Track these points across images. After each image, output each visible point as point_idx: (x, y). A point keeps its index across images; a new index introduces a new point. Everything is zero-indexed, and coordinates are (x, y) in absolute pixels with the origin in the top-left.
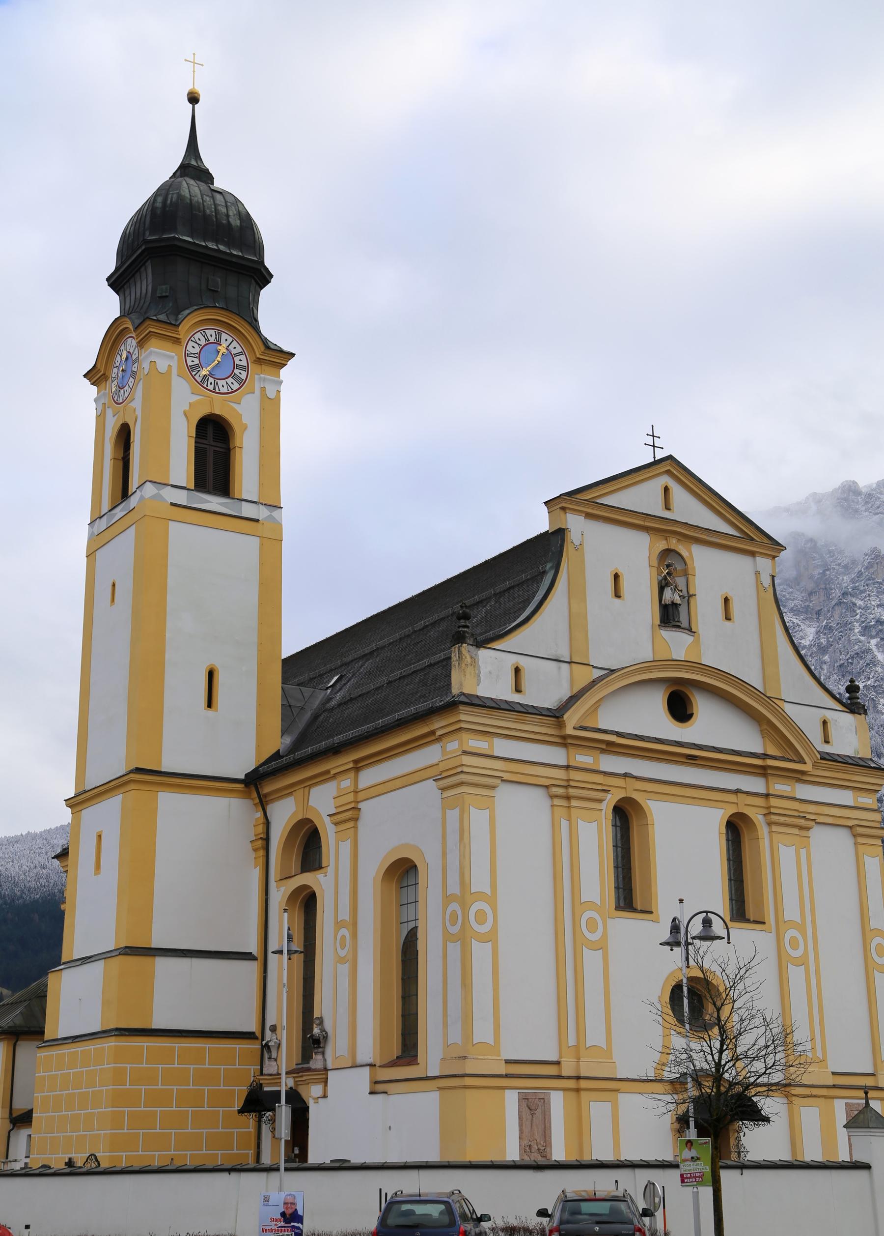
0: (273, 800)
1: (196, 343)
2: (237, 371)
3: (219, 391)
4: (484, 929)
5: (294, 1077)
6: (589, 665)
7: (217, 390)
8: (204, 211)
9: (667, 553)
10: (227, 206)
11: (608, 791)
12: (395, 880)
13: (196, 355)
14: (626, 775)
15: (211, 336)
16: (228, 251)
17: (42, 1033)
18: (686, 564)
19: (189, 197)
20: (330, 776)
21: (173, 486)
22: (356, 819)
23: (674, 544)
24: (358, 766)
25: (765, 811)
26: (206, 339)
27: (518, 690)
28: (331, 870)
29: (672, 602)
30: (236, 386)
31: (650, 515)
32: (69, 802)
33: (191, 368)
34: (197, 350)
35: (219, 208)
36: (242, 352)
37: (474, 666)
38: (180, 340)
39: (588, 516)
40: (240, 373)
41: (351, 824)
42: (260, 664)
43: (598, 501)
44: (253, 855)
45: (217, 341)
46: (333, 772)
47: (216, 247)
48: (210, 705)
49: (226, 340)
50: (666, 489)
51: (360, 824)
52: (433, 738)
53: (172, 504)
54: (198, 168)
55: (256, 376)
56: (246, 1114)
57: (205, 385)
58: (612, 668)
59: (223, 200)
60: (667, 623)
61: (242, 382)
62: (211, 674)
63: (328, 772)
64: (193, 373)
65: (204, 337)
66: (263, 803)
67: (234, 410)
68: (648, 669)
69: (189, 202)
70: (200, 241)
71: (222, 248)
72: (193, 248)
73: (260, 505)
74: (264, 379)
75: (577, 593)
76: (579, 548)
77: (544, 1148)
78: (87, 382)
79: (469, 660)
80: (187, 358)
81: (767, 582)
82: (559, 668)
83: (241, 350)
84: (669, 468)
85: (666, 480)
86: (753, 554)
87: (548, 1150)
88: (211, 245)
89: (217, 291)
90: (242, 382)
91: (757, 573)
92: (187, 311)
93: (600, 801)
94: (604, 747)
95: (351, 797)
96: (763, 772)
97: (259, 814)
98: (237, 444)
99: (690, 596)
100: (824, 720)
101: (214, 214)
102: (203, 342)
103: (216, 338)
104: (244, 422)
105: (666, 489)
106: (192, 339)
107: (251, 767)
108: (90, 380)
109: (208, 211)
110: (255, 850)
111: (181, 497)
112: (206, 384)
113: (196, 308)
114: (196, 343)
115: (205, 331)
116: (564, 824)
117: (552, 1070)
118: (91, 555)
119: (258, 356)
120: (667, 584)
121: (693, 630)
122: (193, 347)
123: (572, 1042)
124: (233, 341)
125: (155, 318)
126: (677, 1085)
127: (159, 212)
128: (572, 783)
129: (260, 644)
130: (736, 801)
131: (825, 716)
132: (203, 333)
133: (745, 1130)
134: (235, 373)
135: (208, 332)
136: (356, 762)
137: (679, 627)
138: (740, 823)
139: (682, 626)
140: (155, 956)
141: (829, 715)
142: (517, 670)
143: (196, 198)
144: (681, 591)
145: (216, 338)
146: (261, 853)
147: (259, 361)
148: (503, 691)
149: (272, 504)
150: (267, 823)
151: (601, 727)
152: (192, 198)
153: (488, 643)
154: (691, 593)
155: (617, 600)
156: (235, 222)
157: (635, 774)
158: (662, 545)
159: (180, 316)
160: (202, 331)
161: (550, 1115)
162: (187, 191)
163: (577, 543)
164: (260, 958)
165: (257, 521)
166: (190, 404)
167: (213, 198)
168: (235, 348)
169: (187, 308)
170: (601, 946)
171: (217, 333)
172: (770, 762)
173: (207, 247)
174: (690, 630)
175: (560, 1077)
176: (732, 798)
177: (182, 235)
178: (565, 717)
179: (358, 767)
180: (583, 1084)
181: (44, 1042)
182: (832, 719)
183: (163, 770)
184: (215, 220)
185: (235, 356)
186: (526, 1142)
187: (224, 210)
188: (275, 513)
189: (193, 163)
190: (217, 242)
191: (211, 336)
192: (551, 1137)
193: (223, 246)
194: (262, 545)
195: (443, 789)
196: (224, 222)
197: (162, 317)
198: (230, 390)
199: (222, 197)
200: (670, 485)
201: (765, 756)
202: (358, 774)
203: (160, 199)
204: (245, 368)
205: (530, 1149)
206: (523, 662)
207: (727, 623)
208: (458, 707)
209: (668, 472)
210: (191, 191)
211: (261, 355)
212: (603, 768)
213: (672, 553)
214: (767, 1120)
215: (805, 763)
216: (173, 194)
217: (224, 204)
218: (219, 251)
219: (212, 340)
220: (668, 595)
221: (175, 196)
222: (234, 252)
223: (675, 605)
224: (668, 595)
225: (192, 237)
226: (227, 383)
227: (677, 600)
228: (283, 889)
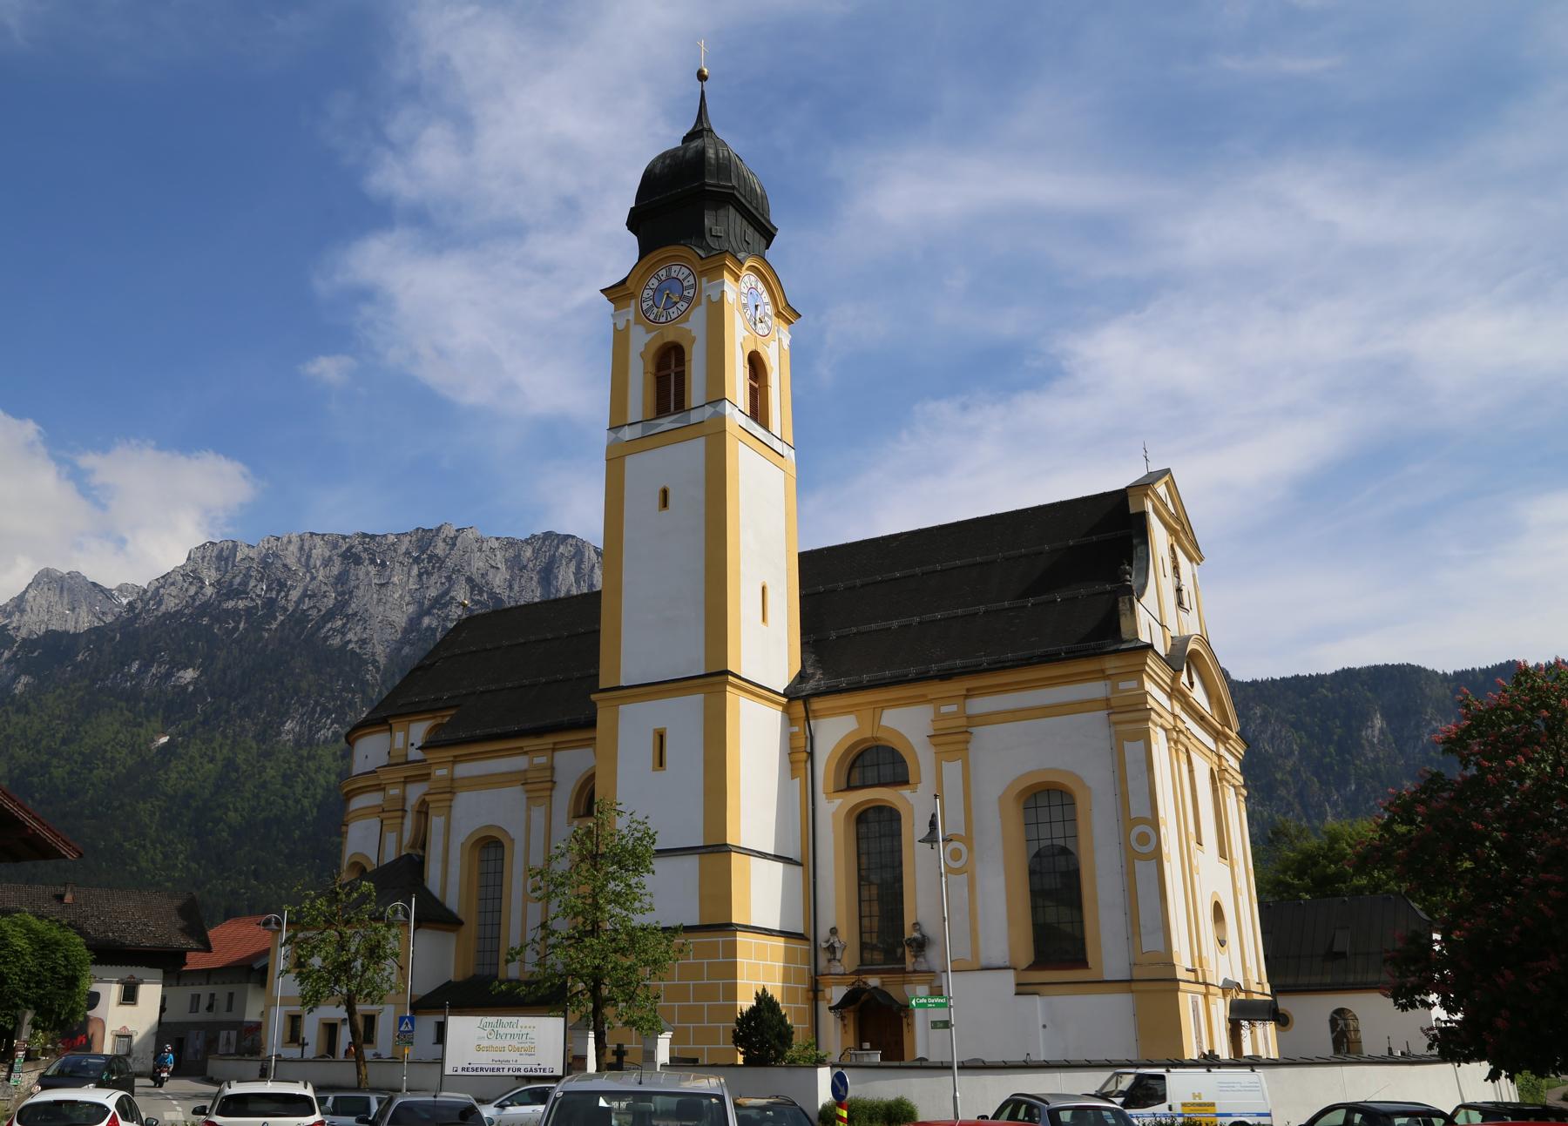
5: (882, 978)
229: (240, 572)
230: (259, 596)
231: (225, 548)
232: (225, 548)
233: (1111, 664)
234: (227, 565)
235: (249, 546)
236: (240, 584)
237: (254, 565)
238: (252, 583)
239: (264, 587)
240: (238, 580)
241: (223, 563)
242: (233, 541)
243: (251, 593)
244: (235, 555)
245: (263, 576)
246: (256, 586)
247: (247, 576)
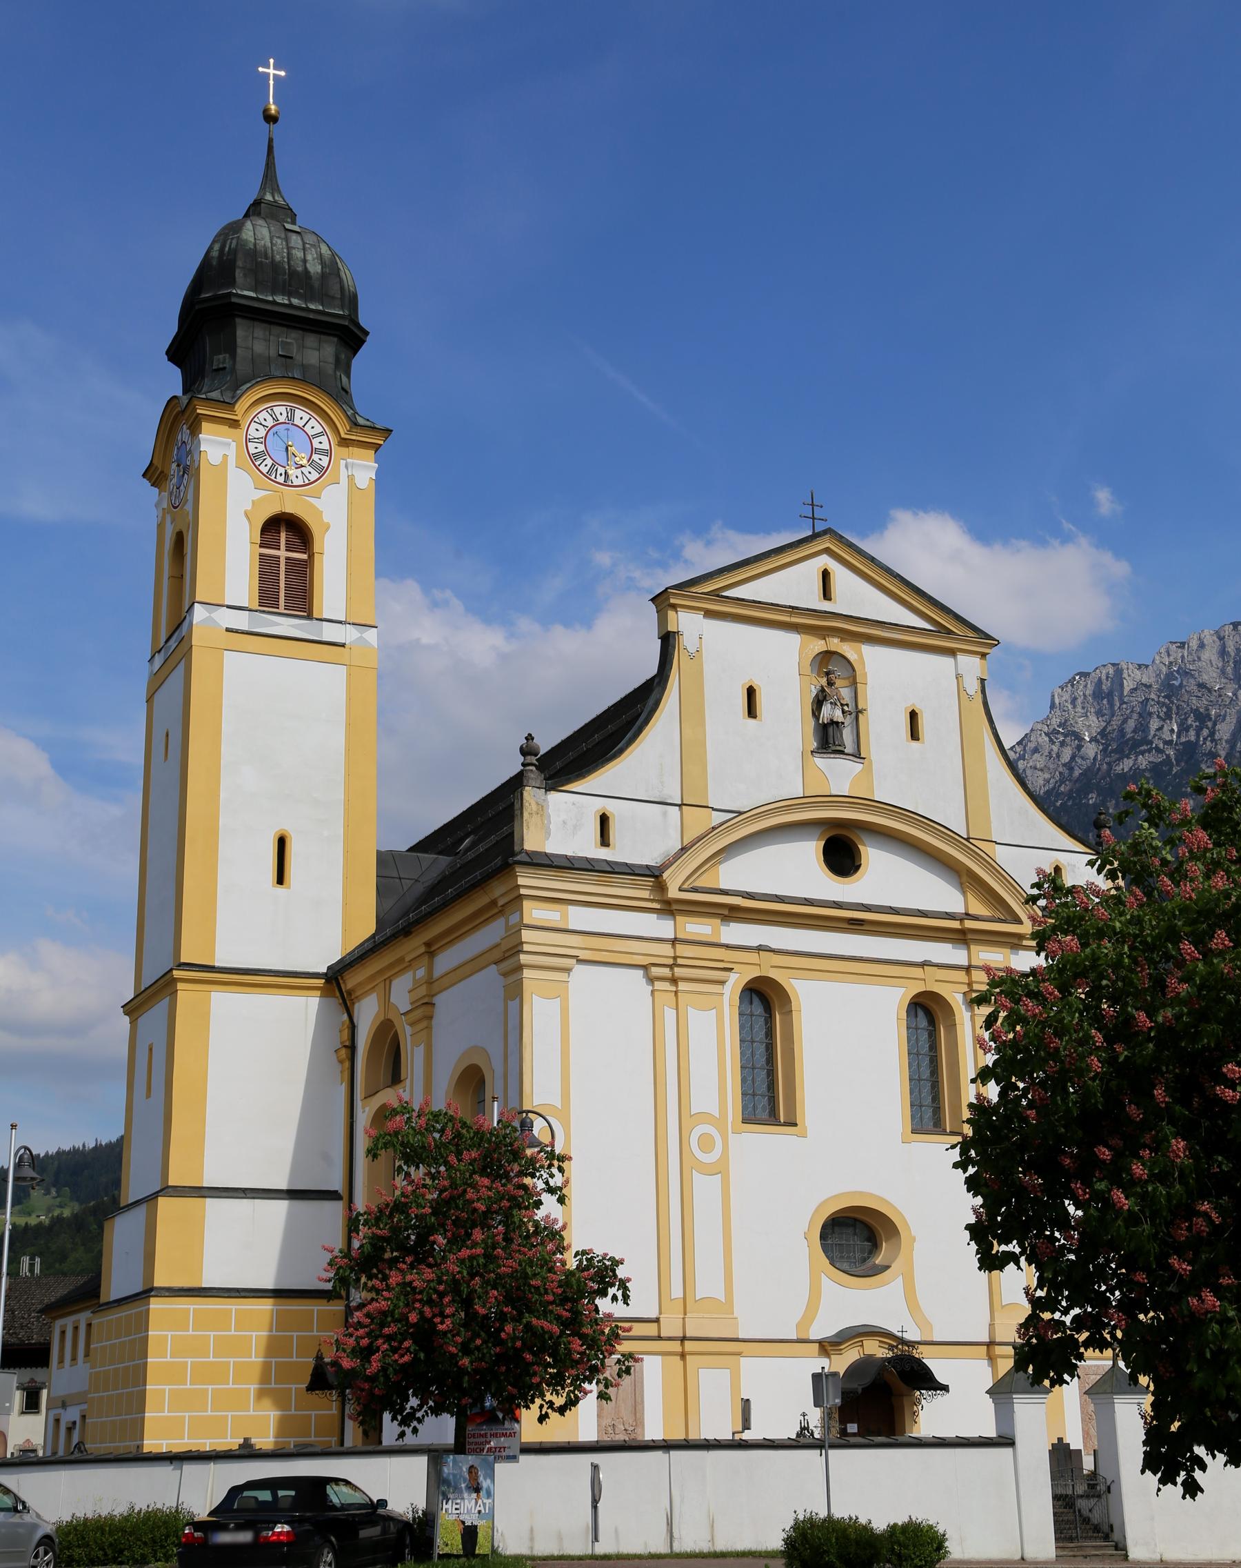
0: (358, 998)
2: (315, 457)
4: (707, 1158)
6: (708, 807)
8: (273, 256)
9: (827, 656)
10: (304, 249)
11: (731, 969)
12: (471, 1091)
14: (760, 949)
15: (281, 414)
16: (304, 306)
17: (98, 1297)
18: (854, 670)
19: (253, 241)
20: (405, 965)
22: (430, 1018)
23: (835, 644)
24: (433, 949)
25: (966, 989)
27: (605, 841)
28: (408, 1082)
29: (832, 720)
30: (315, 475)
31: (797, 608)
32: (127, 1008)
34: (262, 433)
35: (294, 252)
37: (542, 815)
39: (709, 614)
41: (424, 1024)
42: (347, 826)
43: (724, 594)
44: (338, 1067)
46: (407, 959)
47: (286, 302)
48: (280, 880)
49: (301, 418)
50: (826, 575)
51: (434, 1022)
52: (496, 910)
53: (228, 630)
54: (274, 204)
55: (343, 463)
56: (317, 1392)
57: (273, 477)
58: (742, 810)
59: (300, 241)
60: (825, 749)
61: (322, 471)
62: (282, 842)
63: (401, 960)
64: (257, 463)
66: (347, 1003)
67: (312, 506)
68: (788, 809)
69: (252, 247)
70: (266, 296)
71: (295, 301)
72: (256, 305)
73: (348, 625)
74: (353, 464)
75: (692, 716)
76: (696, 656)
77: (633, 1428)
78: (146, 483)
79: (534, 807)
80: (249, 444)
81: (973, 687)
82: (665, 814)
84: (828, 545)
85: (825, 561)
86: (952, 652)
87: (638, 1430)
88: (279, 299)
89: (291, 358)
90: (322, 471)
91: (958, 677)
92: (249, 385)
93: (722, 983)
94: (726, 912)
95: (423, 991)
96: (962, 937)
97: (345, 1017)
98: (316, 549)
99: (861, 712)
100: (1057, 866)
101: (286, 260)
102: (270, 423)
104: (325, 520)
105: (826, 575)
106: (256, 419)
107: (335, 957)
108: (149, 480)
109: (278, 257)
110: (341, 1062)
111: (241, 621)
112: (274, 476)
113: (259, 379)
116: (670, 1014)
117: (651, 1330)
118: (149, 700)
119: (343, 436)
120: (825, 699)
121: (862, 756)
122: (257, 430)
123: (677, 1292)
125: (204, 396)
126: (827, 1346)
127: (214, 263)
128: (680, 961)
129: (347, 802)
130: (923, 977)
131: (1057, 860)
132: (270, 411)
133: (923, 1402)
135: (277, 410)
136: (428, 944)
137: (842, 752)
138: (934, 1007)
139: (846, 751)
140: (205, 1197)
141: (1063, 859)
142: (604, 820)
143: (263, 242)
144: (847, 705)
146: (347, 1064)
147: (344, 443)
148: (585, 845)
149: (363, 623)
150: (353, 1027)
151: (723, 886)
152: (258, 242)
153: (563, 785)
154: (860, 707)
155: (752, 721)
156: (315, 268)
157: (774, 946)
158: (818, 646)
159: (238, 392)
160: (269, 410)
161: (642, 1387)
162: (252, 233)
163: (692, 649)
164: (345, 1196)
165: (343, 645)
166: (253, 502)
167: (287, 240)
168: (313, 428)
169: (249, 381)
170: (720, 1169)
172: (969, 924)
173: (274, 303)
174: (857, 755)
175: (659, 1338)
176: (918, 972)
177: (242, 289)
178: (665, 875)
179: (431, 951)
180: (689, 1346)
181: (100, 1306)
182: (1069, 865)
183: (217, 964)
184: (287, 267)
186: (607, 1421)
187: (300, 254)
189: (269, 197)
190: (290, 295)
191: (281, 414)
192: (643, 1414)
193: (299, 299)
194: (349, 675)
195: (505, 975)
196: (300, 269)
197: (215, 395)
198: (307, 482)
199: (299, 238)
200: (832, 567)
201: (968, 916)
202: (433, 961)
203: (217, 247)
204: (328, 453)
205: (614, 1430)
206: (611, 807)
207: (914, 744)
208: (514, 868)
209: (827, 551)
210: (256, 232)
212: (724, 940)
213: (835, 656)
214: (945, 1388)
215: (1020, 922)
216: (232, 239)
217: (301, 247)
218: (291, 306)
220: (827, 712)
221: (234, 242)
222: (312, 307)
223: (834, 723)
224: (827, 712)
225: (255, 291)
227: (838, 715)
228: (367, 1109)
229: (1132, 712)
230: (1169, 743)
231: (1104, 677)
232: (1104, 677)
233: (497, 890)
234: (1111, 704)
235: (1140, 666)
236: (1134, 731)
237: (1153, 696)
238: (1154, 724)
239: (1175, 728)
240: (1131, 724)
241: (1105, 702)
242: (1113, 665)
243: (1156, 741)
244: (1122, 685)
245: (1169, 709)
246: (1160, 728)
247: (1145, 716)
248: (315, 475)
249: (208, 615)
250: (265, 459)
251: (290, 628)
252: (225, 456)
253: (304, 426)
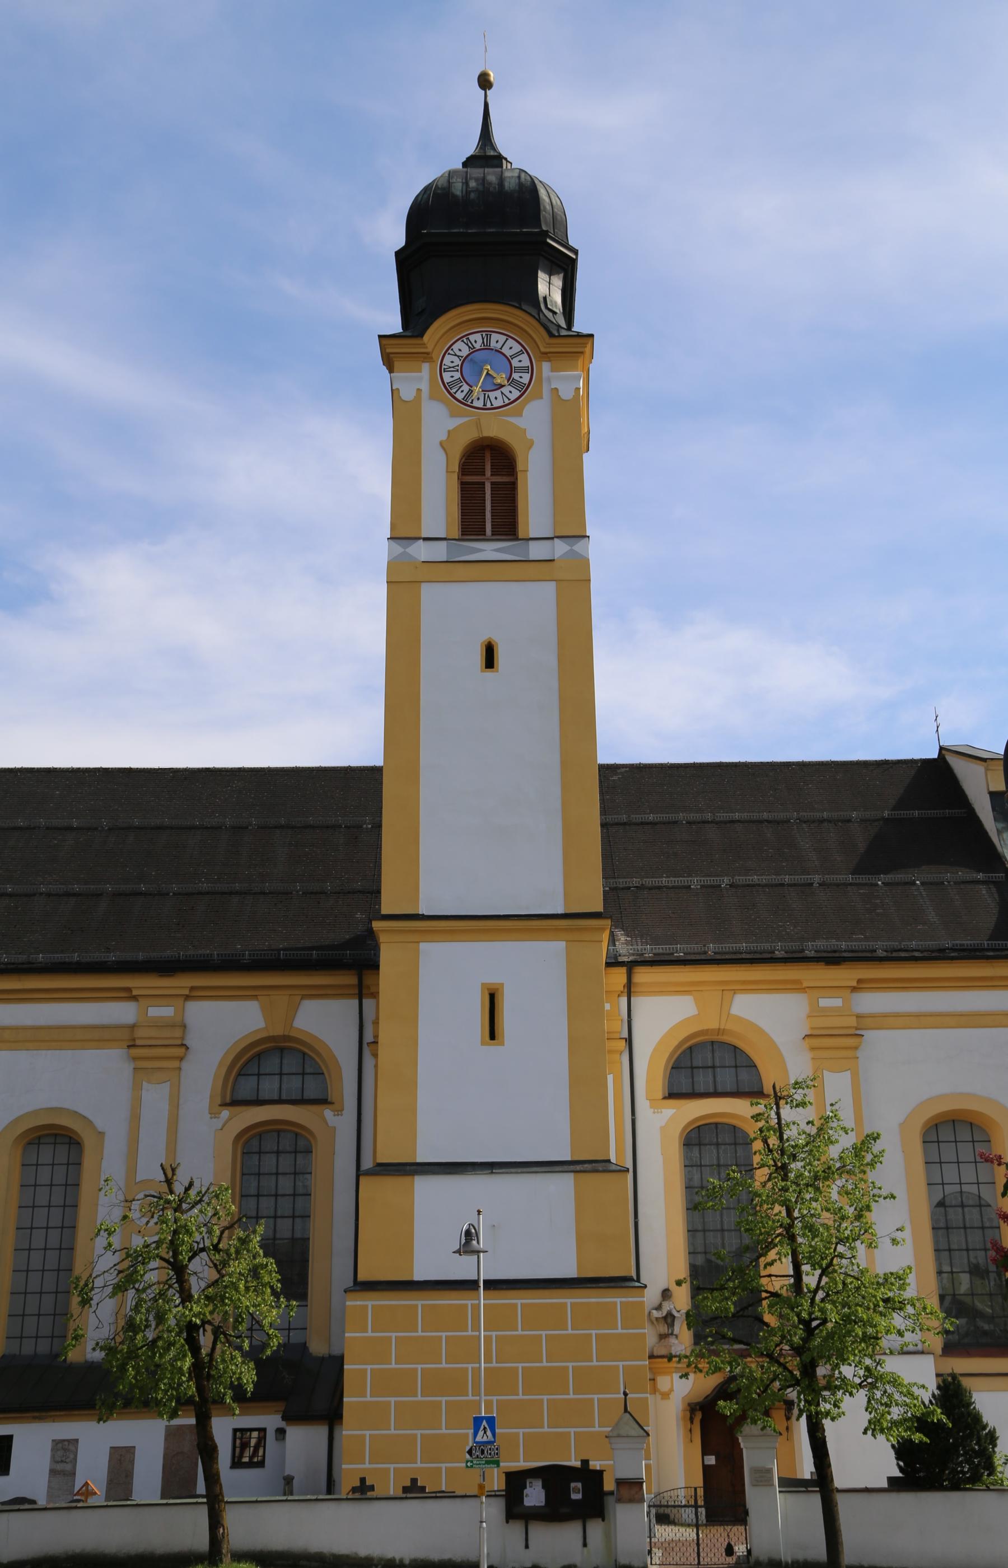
1: (456, 355)
2: (516, 376)
3: (492, 405)
7: (489, 405)
13: (457, 368)
21: (425, 539)
26: (469, 347)
30: (516, 394)
33: (449, 386)
36: (522, 350)
38: (430, 356)
40: (521, 377)
45: (484, 346)
61: (524, 389)
65: (467, 345)
83: (520, 348)
90: (524, 389)
102: (466, 351)
103: (483, 342)
104: (529, 437)
111: (439, 551)
114: (456, 355)
115: (468, 338)
119: (543, 350)
124: (507, 339)
132: (465, 341)
134: (513, 379)
145: (483, 342)
147: (545, 356)
171: (484, 335)
185: (512, 359)
188: (579, 547)
198: (507, 401)
204: (530, 370)
211: (546, 347)
219: (477, 346)
226: (502, 393)
248: (516, 394)
249: (403, 550)
250: (461, 387)
251: (491, 552)
252: (419, 390)
253: (501, 349)
